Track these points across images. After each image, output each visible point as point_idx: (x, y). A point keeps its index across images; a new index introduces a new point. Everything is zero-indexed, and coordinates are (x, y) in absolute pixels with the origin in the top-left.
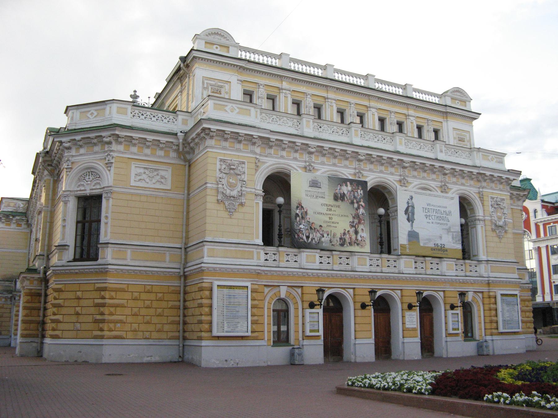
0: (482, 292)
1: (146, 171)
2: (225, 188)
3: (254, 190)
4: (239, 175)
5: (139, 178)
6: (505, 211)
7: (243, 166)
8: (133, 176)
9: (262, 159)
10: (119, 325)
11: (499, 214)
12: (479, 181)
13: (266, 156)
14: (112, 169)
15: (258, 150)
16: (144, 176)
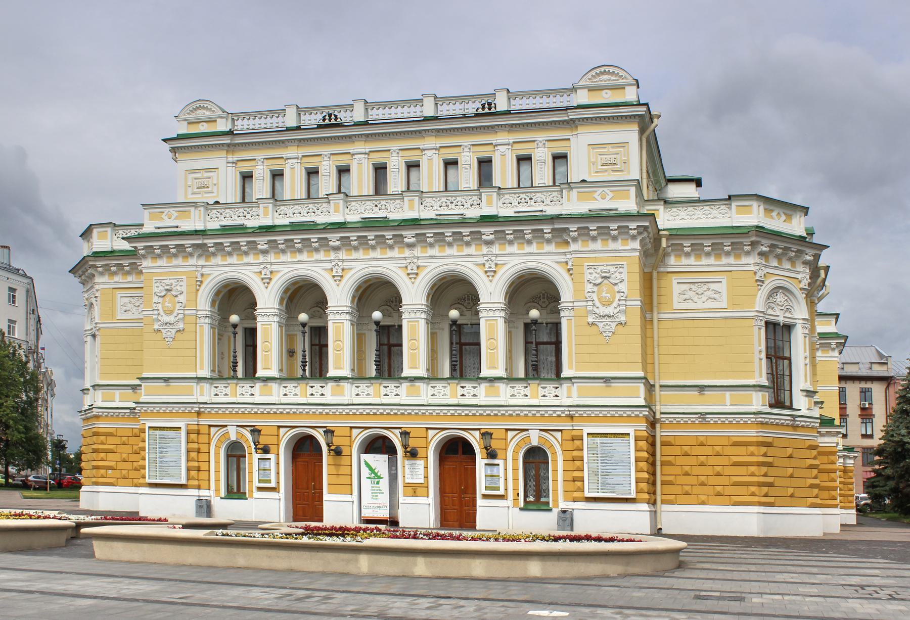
0: (561, 430)
1: (132, 299)
2: (162, 313)
3: (194, 312)
4: (176, 296)
5: (125, 308)
6: (623, 287)
7: (181, 283)
8: (118, 306)
9: (205, 270)
10: (110, 471)
11: (604, 294)
12: (567, 243)
13: (212, 266)
14: (98, 302)
15: (202, 262)
16: (130, 306)
